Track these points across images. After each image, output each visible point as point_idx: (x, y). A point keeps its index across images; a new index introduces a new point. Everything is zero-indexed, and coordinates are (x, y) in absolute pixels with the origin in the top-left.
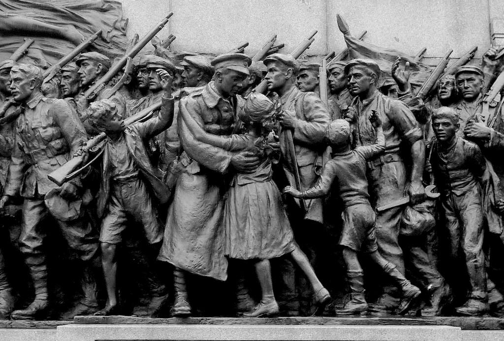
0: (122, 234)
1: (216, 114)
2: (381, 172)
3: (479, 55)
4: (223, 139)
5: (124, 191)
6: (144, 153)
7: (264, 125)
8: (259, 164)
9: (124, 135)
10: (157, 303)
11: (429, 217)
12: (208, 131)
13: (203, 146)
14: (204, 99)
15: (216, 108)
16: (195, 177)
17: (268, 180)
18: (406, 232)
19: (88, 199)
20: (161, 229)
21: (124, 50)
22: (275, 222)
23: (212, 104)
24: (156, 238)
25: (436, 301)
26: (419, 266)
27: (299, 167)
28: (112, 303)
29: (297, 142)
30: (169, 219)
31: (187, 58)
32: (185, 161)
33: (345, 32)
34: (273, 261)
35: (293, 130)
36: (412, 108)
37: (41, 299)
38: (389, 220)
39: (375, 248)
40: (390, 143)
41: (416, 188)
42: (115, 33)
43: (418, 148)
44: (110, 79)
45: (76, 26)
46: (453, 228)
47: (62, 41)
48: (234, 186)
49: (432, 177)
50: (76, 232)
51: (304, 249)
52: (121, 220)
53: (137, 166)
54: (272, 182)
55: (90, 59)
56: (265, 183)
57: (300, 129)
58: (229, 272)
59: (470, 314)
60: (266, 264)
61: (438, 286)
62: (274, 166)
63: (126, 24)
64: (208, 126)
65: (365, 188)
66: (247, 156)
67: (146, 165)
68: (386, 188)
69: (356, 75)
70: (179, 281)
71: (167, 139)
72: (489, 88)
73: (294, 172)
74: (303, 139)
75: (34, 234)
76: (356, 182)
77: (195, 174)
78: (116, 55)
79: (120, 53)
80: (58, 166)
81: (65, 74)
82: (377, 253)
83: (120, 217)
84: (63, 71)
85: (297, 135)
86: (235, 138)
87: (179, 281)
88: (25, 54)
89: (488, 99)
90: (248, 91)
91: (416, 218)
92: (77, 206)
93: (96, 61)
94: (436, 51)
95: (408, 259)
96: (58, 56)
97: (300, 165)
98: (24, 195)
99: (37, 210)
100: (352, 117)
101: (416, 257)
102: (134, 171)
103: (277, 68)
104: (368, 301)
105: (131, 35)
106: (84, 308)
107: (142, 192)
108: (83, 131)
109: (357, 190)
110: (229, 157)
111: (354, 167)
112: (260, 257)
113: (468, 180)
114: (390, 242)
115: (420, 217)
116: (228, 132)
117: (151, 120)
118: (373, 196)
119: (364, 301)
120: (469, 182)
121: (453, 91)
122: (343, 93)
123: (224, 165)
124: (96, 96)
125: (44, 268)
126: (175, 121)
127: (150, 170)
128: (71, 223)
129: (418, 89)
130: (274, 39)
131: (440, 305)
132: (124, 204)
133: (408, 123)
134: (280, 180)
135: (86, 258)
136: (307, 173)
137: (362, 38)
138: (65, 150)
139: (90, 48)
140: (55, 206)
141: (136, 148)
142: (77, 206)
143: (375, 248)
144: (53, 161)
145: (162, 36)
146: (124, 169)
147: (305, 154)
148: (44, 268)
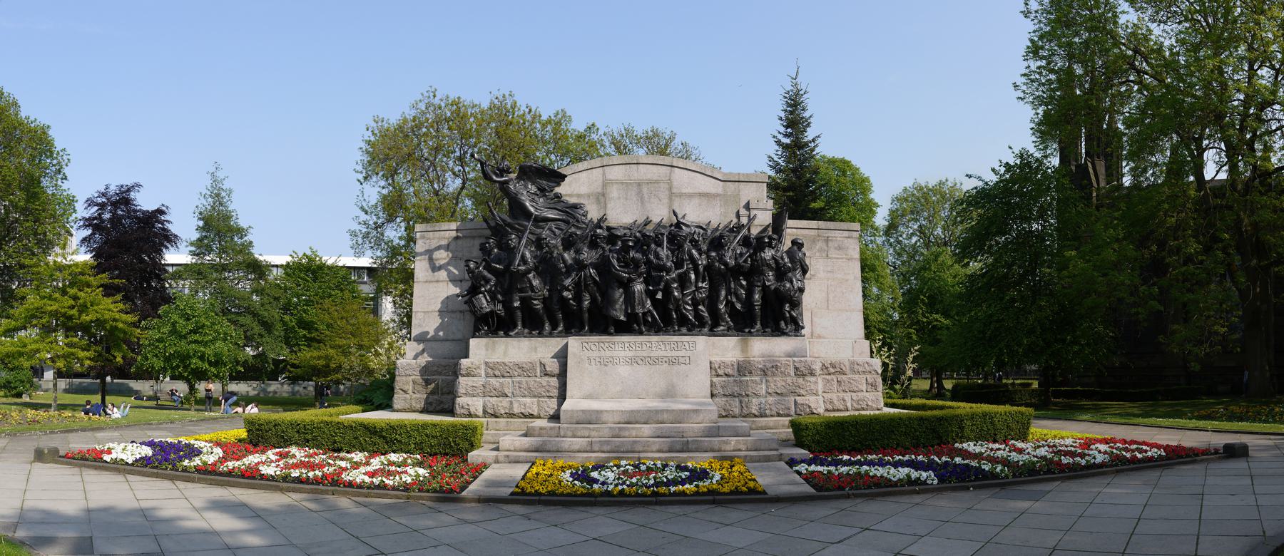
13: (616, 272)
33: (677, 217)
41: (700, 285)
42: (583, 217)
51: (654, 308)
60: (640, 314)
62: (644, 277)
67: (597, 279)
95: (696, 311)
96: (562, 230)
111: (673, 279)
114: (689, 305)
118: (682, 287)
128: (570, 299)
130: (648, 218)
132: (588, 291)
134: (646, 282)
137: (683, 217)
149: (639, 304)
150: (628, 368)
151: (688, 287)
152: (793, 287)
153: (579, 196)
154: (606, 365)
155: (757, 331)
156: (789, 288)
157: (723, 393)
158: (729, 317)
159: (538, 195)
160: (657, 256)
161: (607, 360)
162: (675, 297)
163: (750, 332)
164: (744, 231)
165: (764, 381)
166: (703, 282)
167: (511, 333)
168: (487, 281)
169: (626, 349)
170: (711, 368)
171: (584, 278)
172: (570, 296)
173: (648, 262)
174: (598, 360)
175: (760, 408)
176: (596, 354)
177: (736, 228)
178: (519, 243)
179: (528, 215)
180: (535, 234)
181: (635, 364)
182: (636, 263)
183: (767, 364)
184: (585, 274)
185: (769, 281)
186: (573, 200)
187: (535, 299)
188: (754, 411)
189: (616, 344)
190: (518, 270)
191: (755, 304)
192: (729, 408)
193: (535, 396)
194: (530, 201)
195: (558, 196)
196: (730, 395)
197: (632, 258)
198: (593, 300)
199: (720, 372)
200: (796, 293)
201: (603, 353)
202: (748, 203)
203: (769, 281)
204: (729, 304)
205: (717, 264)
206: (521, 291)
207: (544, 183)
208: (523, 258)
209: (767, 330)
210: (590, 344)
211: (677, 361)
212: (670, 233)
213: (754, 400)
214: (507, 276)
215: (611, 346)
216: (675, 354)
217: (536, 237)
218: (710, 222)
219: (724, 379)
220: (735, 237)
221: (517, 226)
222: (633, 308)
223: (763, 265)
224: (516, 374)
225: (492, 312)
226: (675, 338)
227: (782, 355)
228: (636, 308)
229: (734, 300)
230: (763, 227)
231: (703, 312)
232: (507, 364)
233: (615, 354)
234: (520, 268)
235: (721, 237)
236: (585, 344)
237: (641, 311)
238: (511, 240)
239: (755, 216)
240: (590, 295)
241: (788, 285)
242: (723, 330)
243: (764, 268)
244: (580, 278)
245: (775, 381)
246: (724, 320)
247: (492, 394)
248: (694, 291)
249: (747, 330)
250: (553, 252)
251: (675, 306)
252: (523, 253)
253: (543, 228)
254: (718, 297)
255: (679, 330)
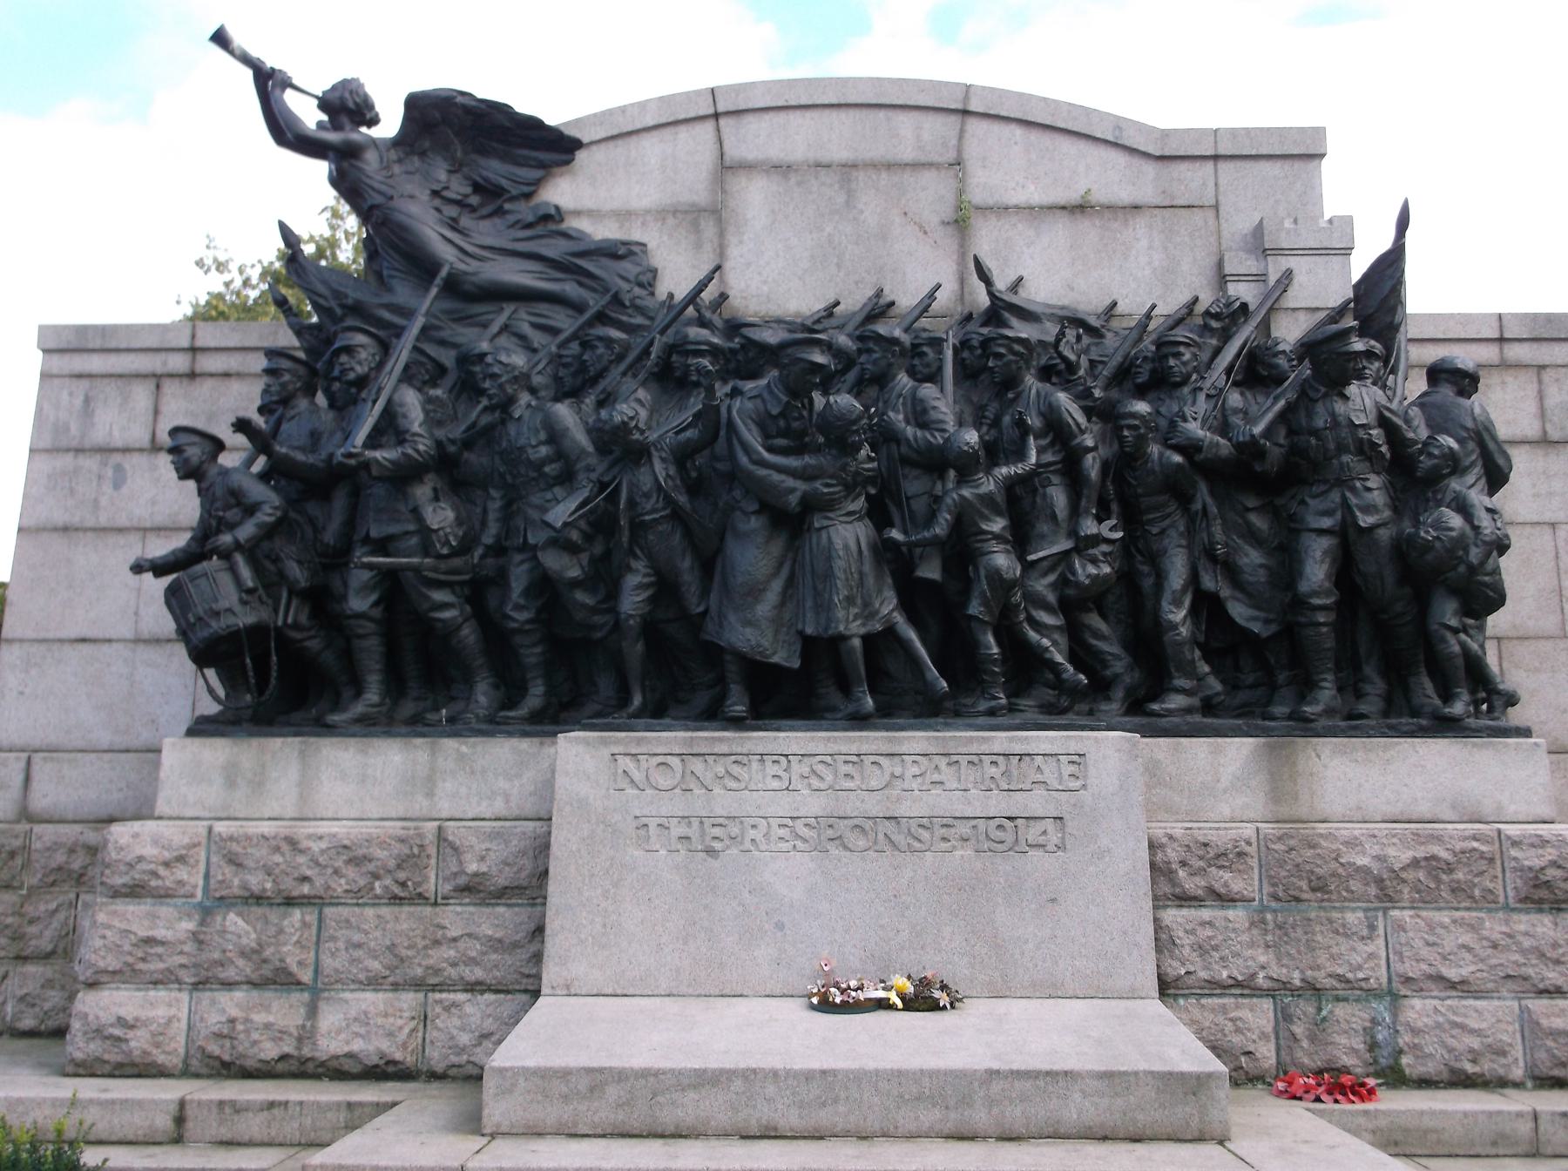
0: (652, 600)
1: (782, 423)
2: (1034, 502)
3: (1200, 308)
4: (792, 462)
5: (651, 537)
6: (678, 482)
7: (850, 440)
8: (846, 497)
9: (650, 456)
10: (702, 699)
11: (1107, 569)
12: (770, 449)
13: (762, 472)
14: (764, 401)
15: (782, 414)
16: (753, 519)
17: (860, 519)
18: (1071, 592)
19: (598, 549)
20: (705, 592)
21: (652, 319)
22: (870, 581)
23: (775, 411)
24: (698, 605)
25: (1119, 693)
26: (1094, 642)
27: (908, 499)
28: (637, 700)
29: (905, 461)
30: (717, 578)
31: (745, 331)
32: (737, 493)
34: (866, 639)
35: (898, 442)
36: (1084, 403)
37: (535, 696)
38: (1045, 574)
39: (1022, 617)
40: (1049, 457)
41: (1089, 527)
42: (637, 291)
43: (1092, 465)
44: (630, 367)
45: (580, 284)
46: (1148, 583)
47: (557, 308)
48: (809, 530)
49: (1114, 507)
50: (581, 596)
51: (914, 619)
52: (646, 580)
53: (669, 500)
54: (867, 521)
55: (600, 338)
56: (856, 524)
57: (907, 440)
58: (806, 656)
59: (1170, 713)
60: (857, 642)
61: (1122, 671)
62: (869, 498)
63: (655, 277)
64: (770, 442)
65: (1004, 528)
66: (828, 485)
67: (682, 499)
68: (1044, 527)
69: (999, 356)
70: (732, 669)
71: (714, 458)
72: (1209, 364)
73: (899, 505)
74: (914, 456)
75: (522, 601)
76: (990, 520)
77: (754, 513)
78: (639, 326)
79: (647, 322)
80: (554, 502)
81: (565, 360)
82: (1025, 625)
83: (645, 575)
84: (561, 356)
85: (904, 449)
86: (809, 459)
87: (732, 669)
88: (505, 328)
89: (1208, 384)
90: (835, 381)
91: (1085, 571)
92: (585, 557)
93: (609, 342)
94: (1132, 304)
95: (1075, 633)
96: (553, 331)
97: (909, 494)
98: (507, 544)
99: (525, 566)
100: (992, 416)
101: (1089, 627)
102: (664, 509)
103: (876, 348)
104: (1008, 697)
105: (662, 291)
106: (597, 707)
107: (677, 538)
108: (591, 449)
109: (992, 533)
110: (801, 486)
111: (987, 500)
112: (848, 633)
113: (1168, 511)
115: (1092, 570)
116: (798, 450)
117: (689, 434)
118: (1020, 539)
119: (1002, 695)
120: (1169, 515)
121: (1153, 371)
122: (982, 377)
123: (794, 499)
124: (609, 395)
125: (538, 650)
126: (723, 433)
127: (688, 507)
128: (575, 584)
129: (1100, 367)
130: (879, 293)
131: (1125, 699)
132: (650, 557)
133: (1074, 427)
134: (878, 515)
135: (599, 635)
136: (919, 506)
138: (567, 478)
139: (601, 318)
140: (554, 561)
141: (668, 475)
142: (585, 557)
143: (1022, 617)
144: (549, 496)
145: (708, 295)
146: (649, 507)
147: (916, 478)
148: (538, 650)
149: (850, 600)
150: (803, 863)
151: (1043, 537)
152: (1476, 529)
153: (625, 215)
154: (710, 852)
155: (1329, 712)
156: (1462, 536)
157: (1203, 974)
158: (1207, 657)
159: (473, 209)
160: (920, 415)
161: (717, 831)
162: (995, 576)
163: (1293, 716)
164: (1245, 334)
165: (1380, 924)
166: (1100, 520)
167: (335, 718)
168: (251, 510)
169: (797, 784)
170: (1153, 865)
171: (632, 503)
172: (574, 573)
173: (885, 437)
174: (678, 830)
175: (1373, 1046)
176: (675, 805)
177: (1217, 316)
178: (380, 365)
179: (422, 266)
180: (455, 346)
181: (835, 851)
182: (839, 435)
183: (1391, 852)
184: (632, 485)
185: (1368, 509)
186: (602, 231)
187: (439, 585)
188: (1347, 1060)
189: (755, 765)
190: (366, 465)
191: (1316, 601)
192: (1237, 1039)
193: (418, 985)
194: (442, 222)
195: (551, 218)
196: (1238, 984)
197: (822, 414)
198: (665, 588)
199: (1192, 885)
200: (1488, 555)
201: (697, 803)
202: (1259, 230)
203: (1368, 509)
204: (1206, 606)
205: (1154, 449)
206: (382, 546)
207: (495, 169)
208: (389, 427)
209: (1363, 708)
210: (644, 765)
211: (1009, 837)
212: (964, 344)
213: (1341, 1011)
214: (340, 502)
215: (736, 769)
216: (998, 804)
217: (453, 353)
218: (1114, 304)
219: (1206, 914)
220: (1217, 352)
221: (387, 315)
222: (823, 607)
223: (1342, 448)
224: (340, 886)
225: (258, 632)
226: (1001, 740)
227: (1448, 814)
228: (841, 614)
229: (1225, 592)
230: (1322, 315)
231: (1102, 637)
232: (304, 844)
233: (749, 803)
234: (369, 454)
235: (1165, 346)
236: (626, 763)
237: (856, 628)
238: (349, 350)
239: (1288, 275)
240: (658, 572)
241: (1456, 521)
242: (1188, 710)
243: (1346, 458)
244: (613, 497)
245: (1431, 927)
246: (1189, 670)
247: (230, 973)
248: (1066, 553)
249: (1280, 710)
250: (511, 400)
251: (997, 614)
252: (389, 401)
253: (485, 326)
254: (1160, 577)
255: (1012, 709)
